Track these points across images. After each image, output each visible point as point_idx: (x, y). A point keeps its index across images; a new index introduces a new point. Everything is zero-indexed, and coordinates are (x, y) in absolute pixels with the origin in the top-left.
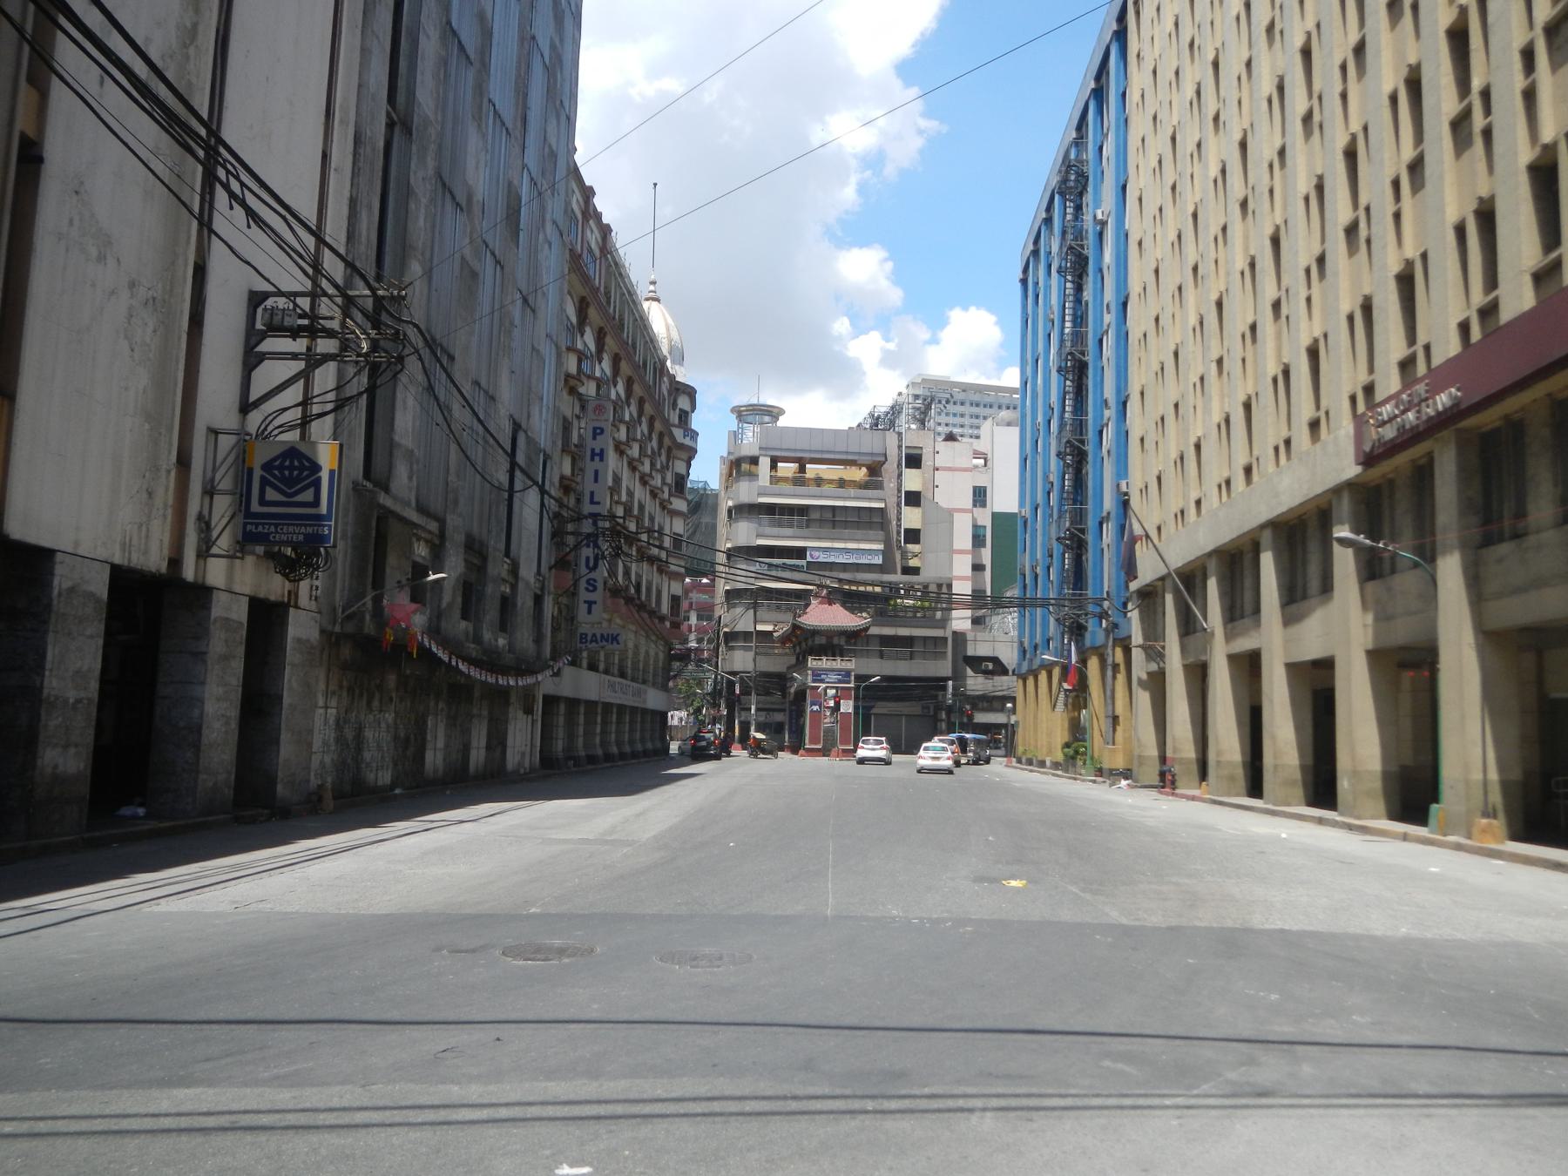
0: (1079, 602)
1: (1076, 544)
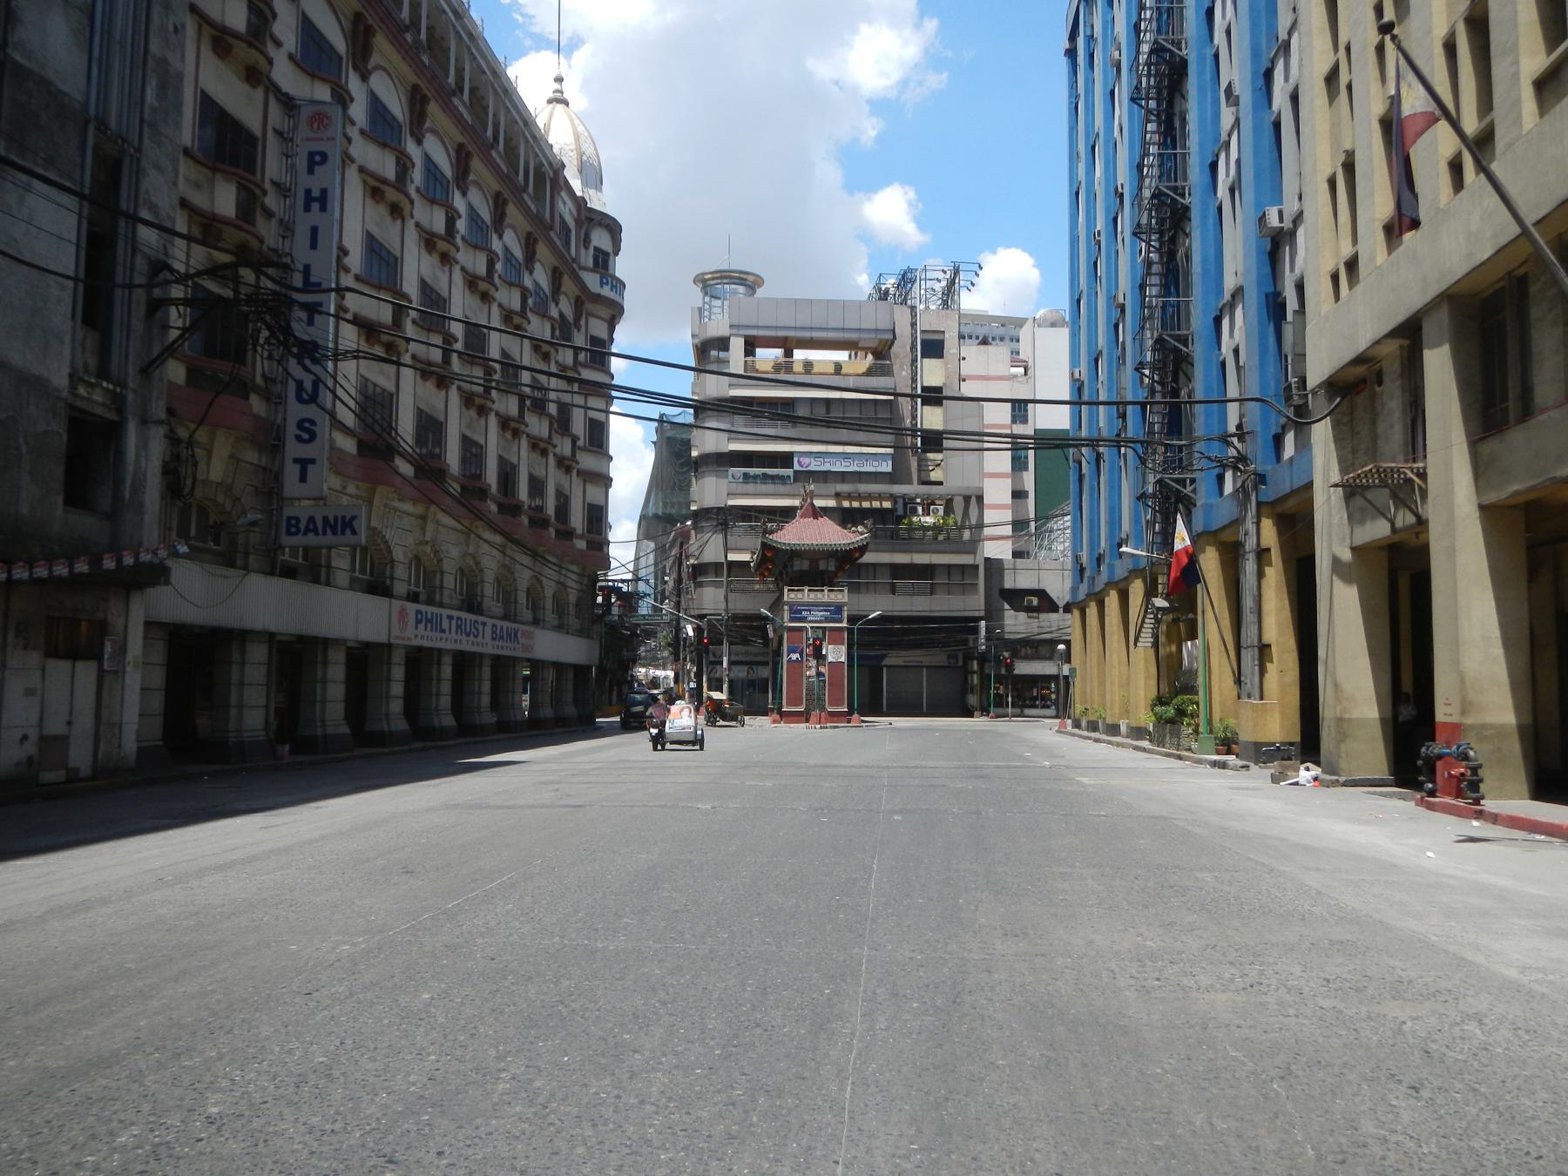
0: (1178, 461)
1: (1172, 362)
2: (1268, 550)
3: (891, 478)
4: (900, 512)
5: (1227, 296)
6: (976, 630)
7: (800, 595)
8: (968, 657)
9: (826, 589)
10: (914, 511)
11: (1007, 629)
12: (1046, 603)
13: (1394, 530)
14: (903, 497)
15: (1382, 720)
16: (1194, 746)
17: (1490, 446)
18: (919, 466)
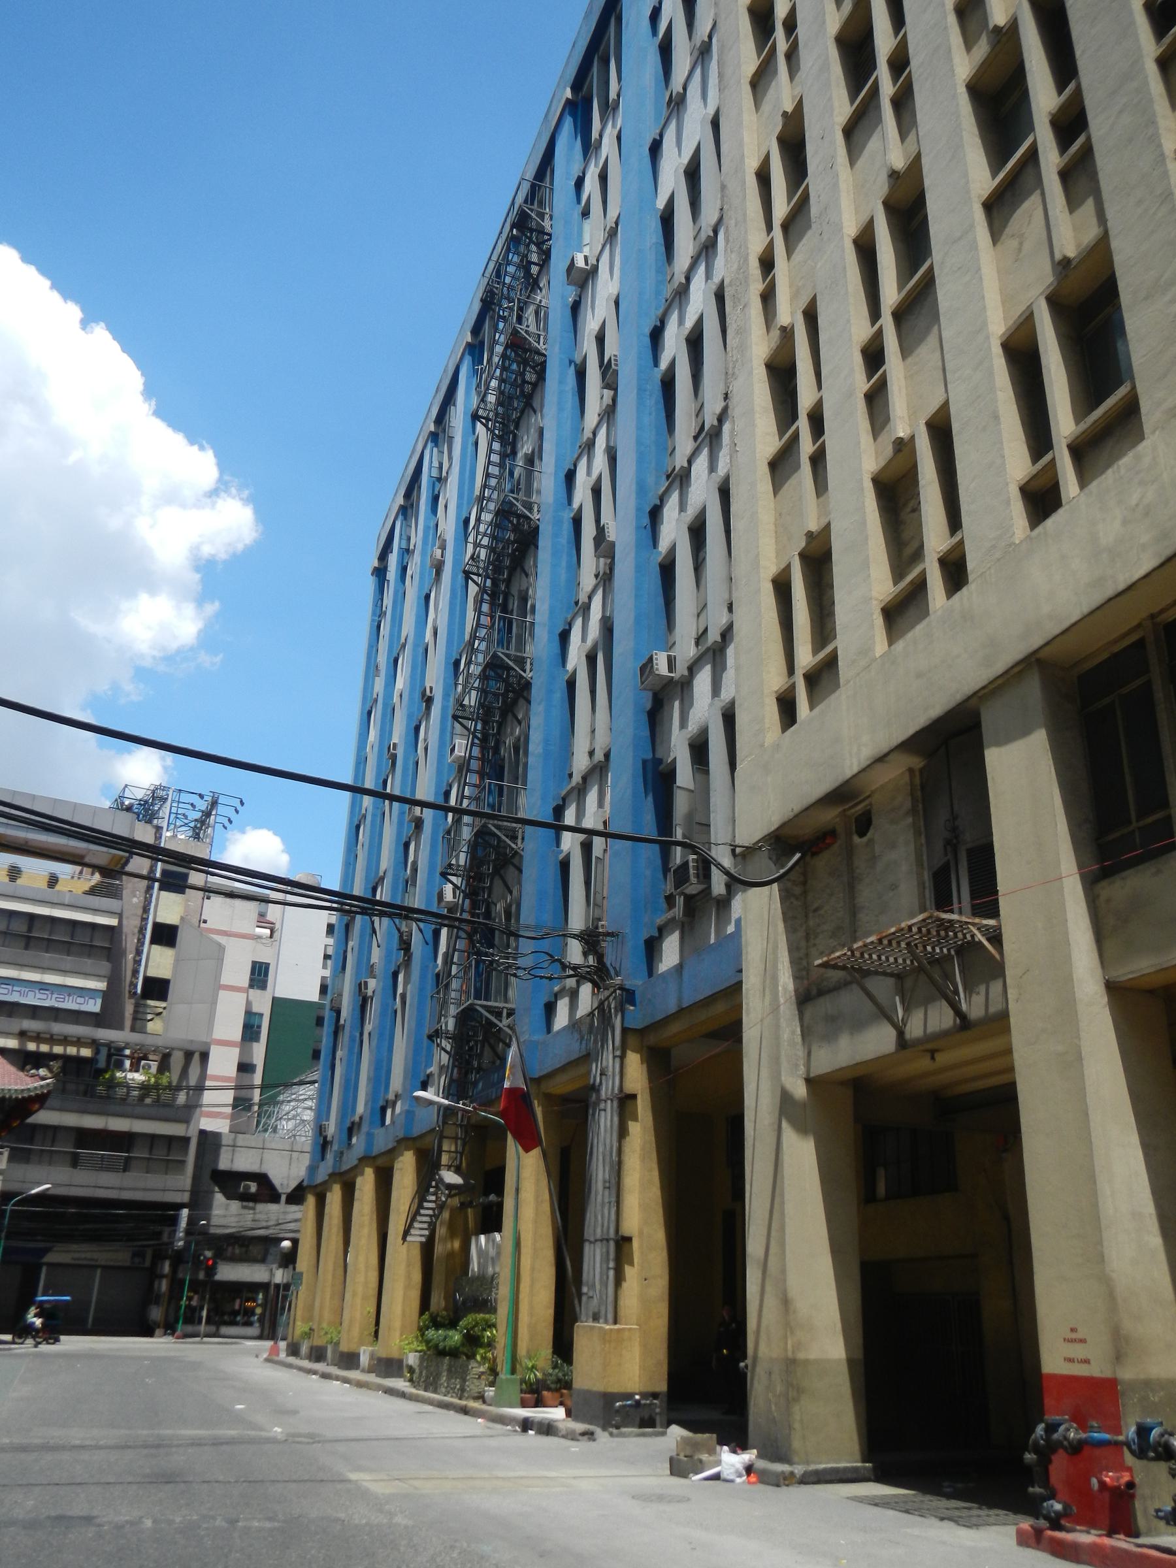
2: (634, 1097)
3: (97, 1020)
4: (102, 1064)
5: (577, 779)
6: (174, 1221)
8: (159, 1257)
10: (120, 1066)
11: (214, 1221)
12: (266, 1190)
13: (902, 1042)
14: (109, 1045)
15: (851, 1362)
16: (490, 1392)
17: (1120, 889)
18: (136, 1012)
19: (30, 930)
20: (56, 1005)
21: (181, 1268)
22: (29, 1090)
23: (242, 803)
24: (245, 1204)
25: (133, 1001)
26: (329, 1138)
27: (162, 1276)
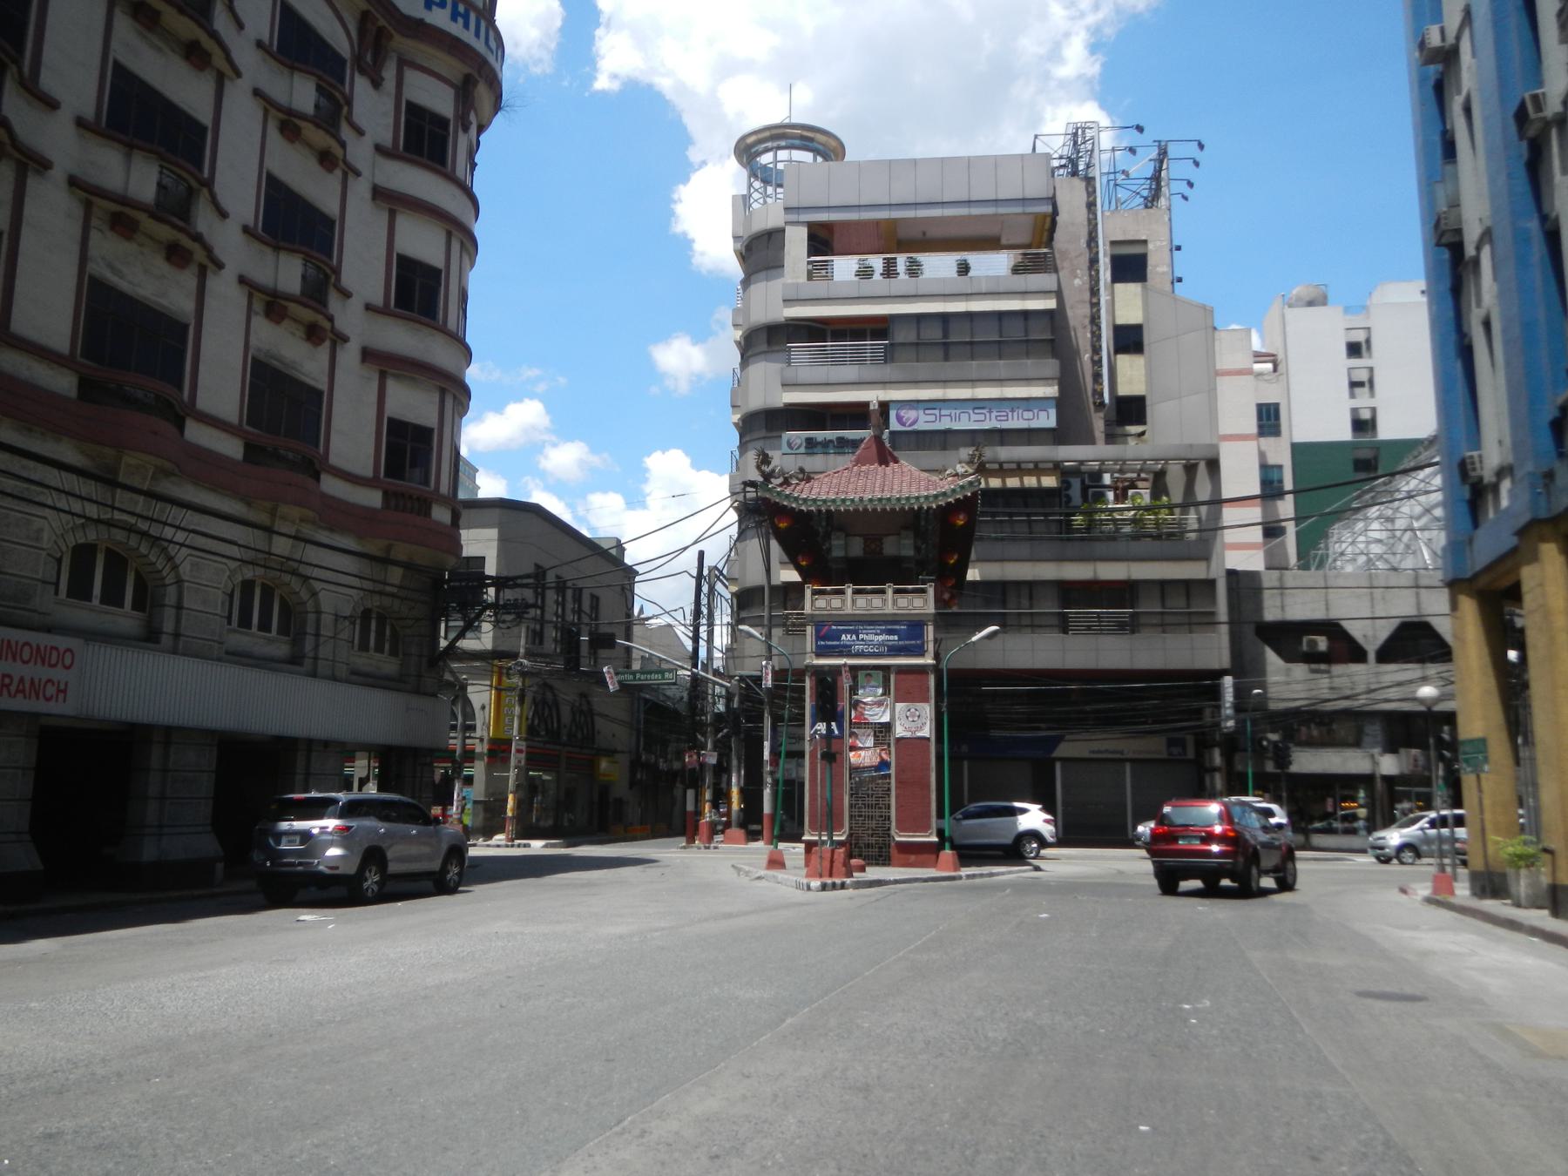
3: (1057, 436)
6: (1215, 693)
7: (836, 602)
8: (1204, 743)
9: (890, 588)
10: (1100, 497)
11: (1273, 692)
12: (1345, 648)
14: (1076, 472)
19: (946, 334)
20: (999, 425)
21: (1237, 757)
22: (944, 494)
23: (1201, 146)
24: (1314, 666)
25: (1101, 415)
26: (1488, 476)
27: (1215, 769)
